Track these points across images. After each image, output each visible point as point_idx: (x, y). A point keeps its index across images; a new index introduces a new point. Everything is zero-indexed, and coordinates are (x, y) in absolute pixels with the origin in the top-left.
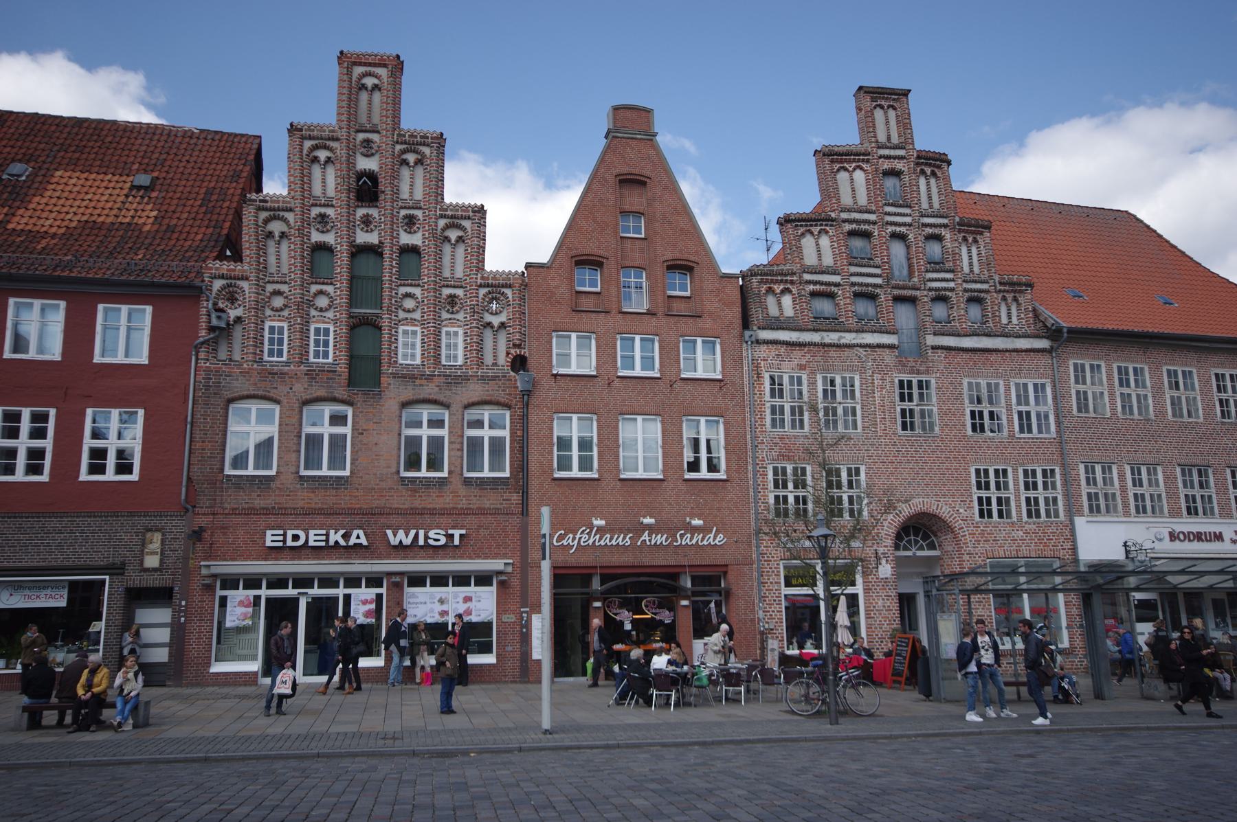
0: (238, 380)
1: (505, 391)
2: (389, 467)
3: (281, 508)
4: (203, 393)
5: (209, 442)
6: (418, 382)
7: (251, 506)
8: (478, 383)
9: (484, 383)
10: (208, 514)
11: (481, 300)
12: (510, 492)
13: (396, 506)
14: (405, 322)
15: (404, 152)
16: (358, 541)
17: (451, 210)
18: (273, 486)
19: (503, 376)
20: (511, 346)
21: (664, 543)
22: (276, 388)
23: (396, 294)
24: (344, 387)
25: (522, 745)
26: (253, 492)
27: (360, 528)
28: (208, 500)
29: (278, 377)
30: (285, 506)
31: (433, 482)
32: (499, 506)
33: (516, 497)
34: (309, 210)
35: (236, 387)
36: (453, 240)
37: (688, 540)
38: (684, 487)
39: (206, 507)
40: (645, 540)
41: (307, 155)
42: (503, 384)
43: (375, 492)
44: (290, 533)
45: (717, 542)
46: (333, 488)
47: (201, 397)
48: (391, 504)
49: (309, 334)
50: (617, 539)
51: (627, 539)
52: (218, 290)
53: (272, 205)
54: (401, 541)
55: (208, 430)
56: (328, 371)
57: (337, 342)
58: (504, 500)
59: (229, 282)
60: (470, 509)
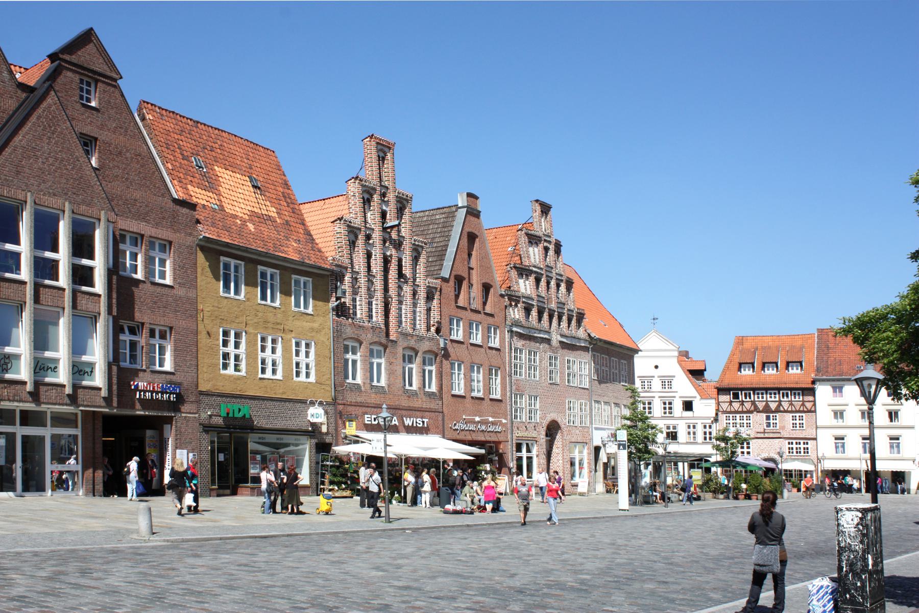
6: (409, 338)
16: (395, 423)
38: (489, 402)
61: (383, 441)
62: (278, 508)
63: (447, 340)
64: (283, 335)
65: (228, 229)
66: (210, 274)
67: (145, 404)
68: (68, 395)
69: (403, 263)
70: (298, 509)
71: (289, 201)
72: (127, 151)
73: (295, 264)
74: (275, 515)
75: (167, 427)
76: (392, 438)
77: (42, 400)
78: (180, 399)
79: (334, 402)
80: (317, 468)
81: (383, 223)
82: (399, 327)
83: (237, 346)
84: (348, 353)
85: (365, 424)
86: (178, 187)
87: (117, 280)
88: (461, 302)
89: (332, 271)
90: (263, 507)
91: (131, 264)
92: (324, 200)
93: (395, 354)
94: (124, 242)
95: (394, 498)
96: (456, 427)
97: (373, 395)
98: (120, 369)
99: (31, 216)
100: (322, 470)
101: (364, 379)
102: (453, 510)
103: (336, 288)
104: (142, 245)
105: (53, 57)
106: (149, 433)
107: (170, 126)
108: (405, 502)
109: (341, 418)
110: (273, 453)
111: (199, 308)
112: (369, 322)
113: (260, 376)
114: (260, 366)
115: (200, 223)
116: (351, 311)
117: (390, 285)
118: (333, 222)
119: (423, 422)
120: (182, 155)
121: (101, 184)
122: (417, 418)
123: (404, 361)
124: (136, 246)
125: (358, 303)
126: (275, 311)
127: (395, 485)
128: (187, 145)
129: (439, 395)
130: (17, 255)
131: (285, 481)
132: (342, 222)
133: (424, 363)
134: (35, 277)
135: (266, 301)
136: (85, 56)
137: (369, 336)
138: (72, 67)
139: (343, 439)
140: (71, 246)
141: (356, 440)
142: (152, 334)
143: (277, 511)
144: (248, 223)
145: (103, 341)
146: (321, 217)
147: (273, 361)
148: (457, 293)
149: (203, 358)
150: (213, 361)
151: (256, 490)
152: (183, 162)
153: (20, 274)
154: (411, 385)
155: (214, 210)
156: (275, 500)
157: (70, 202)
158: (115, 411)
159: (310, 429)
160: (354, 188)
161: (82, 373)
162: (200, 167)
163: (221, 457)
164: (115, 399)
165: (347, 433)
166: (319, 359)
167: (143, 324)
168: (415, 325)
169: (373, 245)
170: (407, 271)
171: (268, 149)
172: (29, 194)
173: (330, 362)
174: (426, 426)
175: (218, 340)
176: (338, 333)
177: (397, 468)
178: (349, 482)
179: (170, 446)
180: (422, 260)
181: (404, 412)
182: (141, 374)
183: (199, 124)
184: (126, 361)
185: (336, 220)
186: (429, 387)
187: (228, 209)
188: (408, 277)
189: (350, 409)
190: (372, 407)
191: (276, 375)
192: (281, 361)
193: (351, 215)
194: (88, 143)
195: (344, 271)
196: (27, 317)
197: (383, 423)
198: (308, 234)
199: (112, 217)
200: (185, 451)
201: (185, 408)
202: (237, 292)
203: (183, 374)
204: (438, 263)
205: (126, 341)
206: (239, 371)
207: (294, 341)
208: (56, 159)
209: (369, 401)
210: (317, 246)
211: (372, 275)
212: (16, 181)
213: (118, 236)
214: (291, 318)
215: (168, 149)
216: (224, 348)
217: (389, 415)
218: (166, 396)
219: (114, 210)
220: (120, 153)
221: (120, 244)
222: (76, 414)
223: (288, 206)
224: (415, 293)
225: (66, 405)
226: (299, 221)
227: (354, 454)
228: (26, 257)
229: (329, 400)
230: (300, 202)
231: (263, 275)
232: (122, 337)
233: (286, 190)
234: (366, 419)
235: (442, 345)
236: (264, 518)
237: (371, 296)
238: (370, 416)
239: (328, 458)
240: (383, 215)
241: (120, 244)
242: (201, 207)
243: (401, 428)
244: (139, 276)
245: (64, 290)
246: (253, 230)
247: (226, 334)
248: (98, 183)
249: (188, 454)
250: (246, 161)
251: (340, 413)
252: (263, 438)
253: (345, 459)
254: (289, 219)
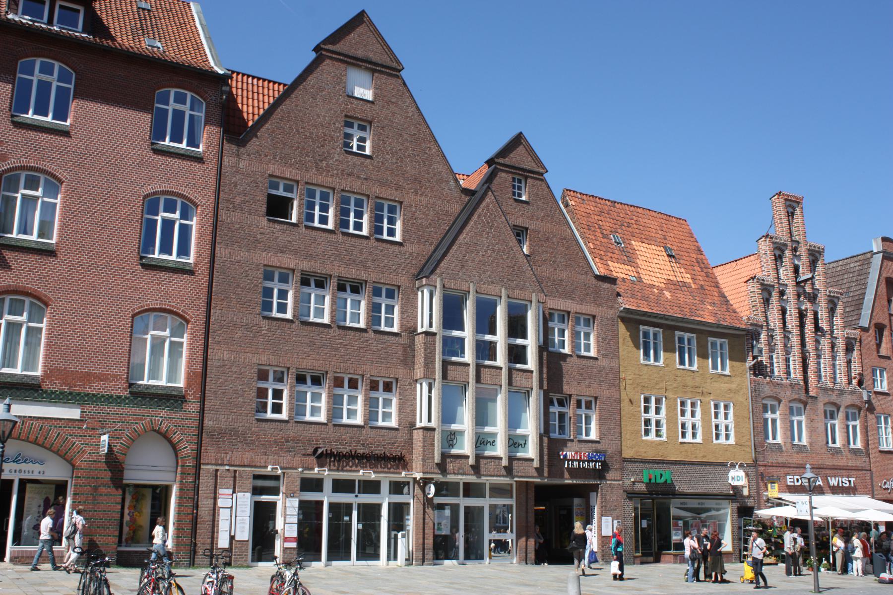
6: (830, 393)
61: (808, 503)
62: (702, 576)
63: (870, 392)
64: (701, 398)
65: (645, 299)
66: (630, 343)
67: (573, 473)
68: (505, 467)
69: (819, 316)
70: (722, 577)
71: (703, 266)
72: (554, 236)
73: (711, 327)
74: (699, 584)
75: (593, 495)
76: (817, 499)
77: (482, 473)
78: (605, 467)
79: (755, 464)
80: (739, 533)
81: (796, 278)
82: (819, 382)
83: (658, 411)
84: (767, 412)
85: (788, 486)
86: (599, 264)
87: (547, 356)
88: (884, 351)
89: (748, 331)
90: (686, 575)
91: (559, 340)
92: (736, 261)
93: (815, 411)
94: (552, 320)
95: (822, 565)
96: (886, 486)
97: (795, 455)
98: (550, 440)
99: (473, 304)
100: (744, 535)
101: (785, 436)
102: (890, 579)
103: (753, 347)
104: (568, 322)
105: (490, 162)
106: (577, 501)
107: (590, 209)
108: (835, 570)
109: (762, 480)
110: (694, 518)
111: (621, 377)
112: (787, 379)
113: (681, 440)
114: (680, 430)
115: (620, 296)
116: (768, 370)
117: (807, 340)
118: (746, 282)
119: (850, 481)
120: (602, 233)
121: (532, 269)
122: (842, 477)
123: (826, 417)
124: (564, 322)
125: (775, 360)
126: (693, 375)
127: (822, 551)
128: (606, 224)
129: (866, 452)
130: (462, 340)
131: (708, 547)
132: (755, 281)
133: (847, 418)
134: (477, 359)
135: (684, 365)
136: (516, 158)
137: (788, 393)
138: (504, 168)
139: (765, 502)
140: (507, 328)
141: (779, 503)
142: (579, 405)
143: (701, 579)
144: (664, 292)
145: (535, 414)
146: (733, 278)
147: (692, 424)
148: (878, 342)
149: (626, 426)
150: (636, 427)
151: (678, 557)
152: (603, 240)
153: (464, 357)
154: (834, 442)
155: (633, 282)
156: (699, 567)
157: (506, 288)
158: (546, 480)
159: (731, 492)
160: (765, 246)
161: (516, 446)
162: (618, 243)
163: (644, 524)
164: (546, 469)
165: (769, 496)
166: (739, 420)
167: (570, 396)
168: (835, 378)
169: (787, 301)
170: (824, 324)
171: (680, 219)
172: (471, 284)
173: (749, 423)
174: (853, 485)
175: (640, 407)
176: (756, 393)
177: (824, 532)
178: (773, 548)
179: (596, 513)
180: (839, 311)
181: (828, 472)
182: (569, 444)
183: (616, 204)
184: (555, 433)
185: (749, 280)
186: (854, 444)
187: (646, 279)
188: (825, 329)
189: (771, 470)
190: (794, 467)
191: (696, 438)
192: (700, 424)
193: (764, 273)
194: (520, 233)
195: (759, 329)
196: (470, 395)
197: (807, 484)
198: (723, 296)
199: (542, 297)
200: (610, 519)
201: (610, 475)
202: (656, 359)
203: (608, 442)
204: (856, 313)
205: (555, 413)
206: (660, 436)
207: (712, 403)
208: (494, 251)
210: (731, 307)
211: (787, 331)
212: (461, 274)
213: (547, 315)
214: (709, 381)
215: (589, 230)
216: (646, 415)
217: (813, 475)
218: (592, 465)
219: (543, 291)
220: (548, 239)
221: (549, 322)
222: (511, 485)
223: (702, 271)
224: (833, 346)
225: (503, 476)
226: (713, 284)
227: (777, 517)
228: (469, 340)
229: (750, 462)
230: (712, 265)
231: (681, 340)
232: (552, 409)
233: (700, 256)
234: (789, 480)
235: (865, 398)
236: (688, 587)
237: (787, 351)
238: (792, 477)
239: (750, 523)
240: (796, 269)
241: (549, 322)
242: (621, 280)
243: (826, 489)
244: (567, 350)
245: (501, 368)
246: (669, 297)
247: (647, 400)
248: (530, 269)
249: (613, 521)
250: (660, 232)
251: (762, 474)
252: (685, 503)
253: (768, 524)
254: (703, 283)
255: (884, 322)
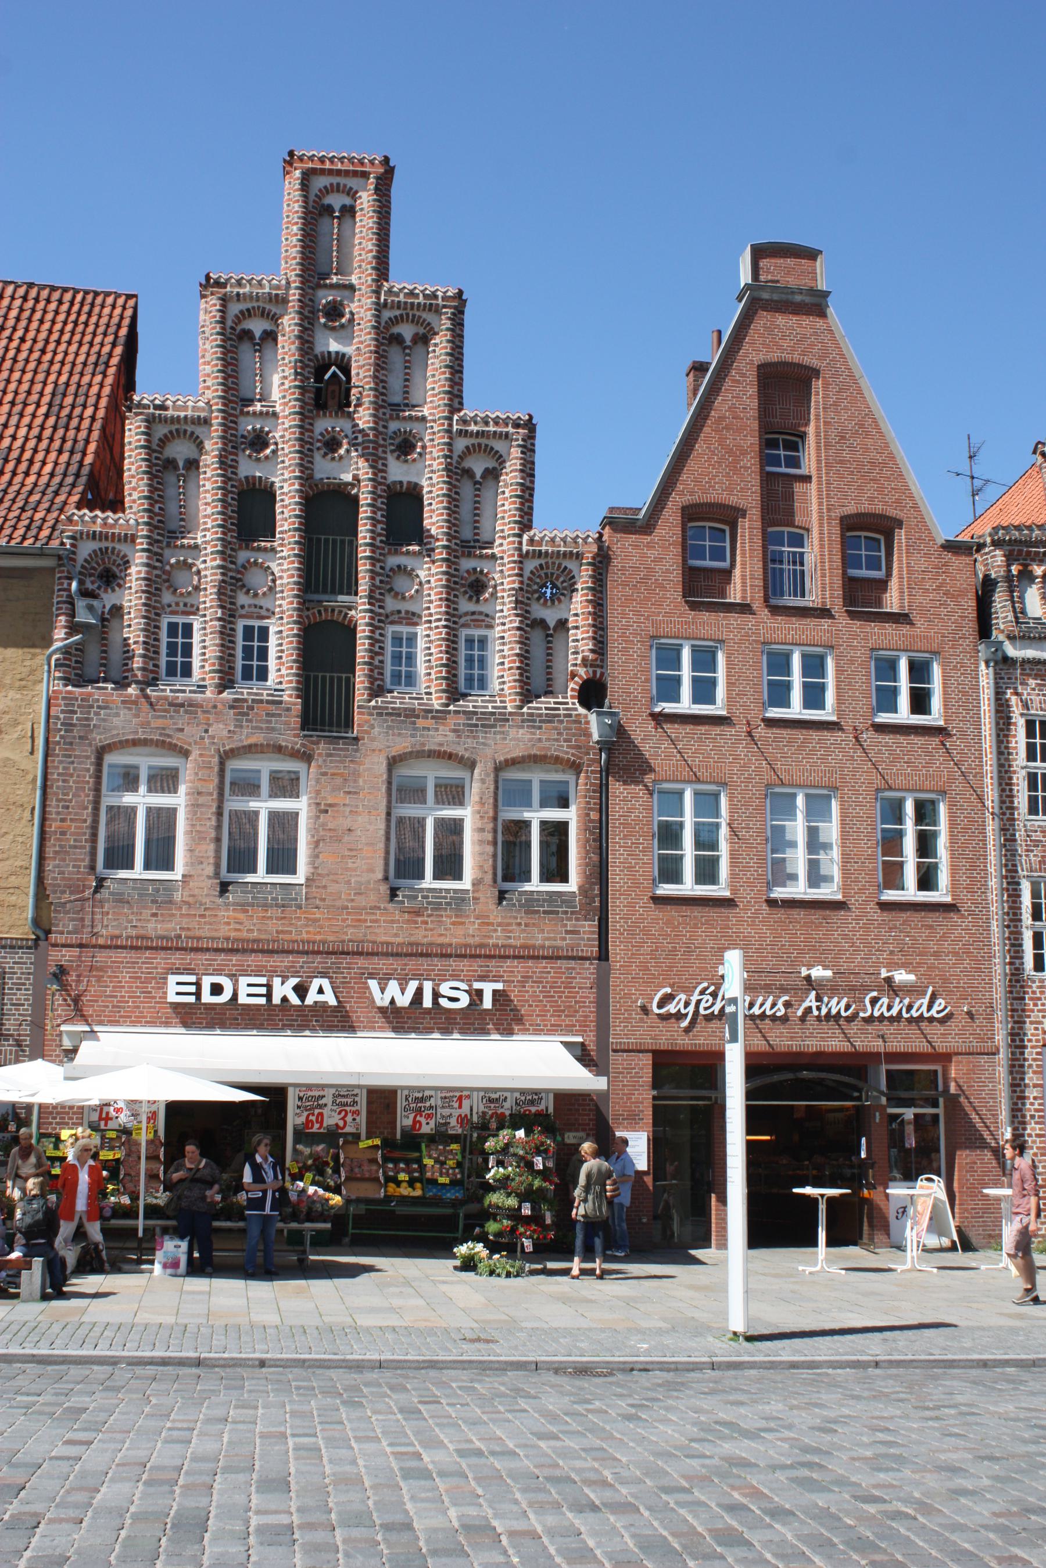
0: (117, 715)
1: (569, 741)
2: (371, 870)
3: (193, 938)
4: (61, 737)
5: (72, 820)
6: (421, 723)
7: (142, 932)
8: (522, 727)
9: (534, 727)
10: (71, 946)
11: (526, 581)
12: (577, 919)
13: (384, 939)
14: (395, 617)
15: (396, 321)
16: (321, 998)
17: (476, 423)
18: (178, 896)
19: (565, 716)
20: (579, 662)
21: (843, 1014)
22: (182, 730)
23: (382, 568)
24: (294, 729)
25: (714, 1359)
26: (145, 908)
27: (324, 975)
28: (73, 920)
29: (186, 712)
30: (198, 933)
31: (445, 898)
32: (559, 943)
33: (589, 928)
34: (235, 423)
35: (116, 728)
36: (478, 473)
37: (884, 1009)
38: (878, 915)
39: (69, 933)
40: (810, 1008)
41: (232, 328)
42: (566, 728)
43: (348, 914)
44: (207, 982)
45: (933, 1012)
46: (277, 905)
47: (58, 743)
48: (376, 934)
49: (234, 636)
50: (761, 1005)
51: (780, 1005)
52: (86, 560)
53: (176, 414)
54: (392, 1001)
55: (70, 801)
56: (268, 702)
57: (282, 651)
58: (567, 932)
59: (104, 544)
60: (510, 946)
209: (205, 932)
255: (733, 500)
